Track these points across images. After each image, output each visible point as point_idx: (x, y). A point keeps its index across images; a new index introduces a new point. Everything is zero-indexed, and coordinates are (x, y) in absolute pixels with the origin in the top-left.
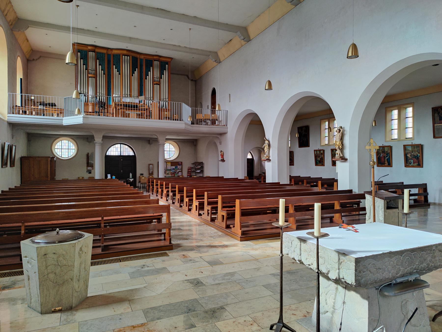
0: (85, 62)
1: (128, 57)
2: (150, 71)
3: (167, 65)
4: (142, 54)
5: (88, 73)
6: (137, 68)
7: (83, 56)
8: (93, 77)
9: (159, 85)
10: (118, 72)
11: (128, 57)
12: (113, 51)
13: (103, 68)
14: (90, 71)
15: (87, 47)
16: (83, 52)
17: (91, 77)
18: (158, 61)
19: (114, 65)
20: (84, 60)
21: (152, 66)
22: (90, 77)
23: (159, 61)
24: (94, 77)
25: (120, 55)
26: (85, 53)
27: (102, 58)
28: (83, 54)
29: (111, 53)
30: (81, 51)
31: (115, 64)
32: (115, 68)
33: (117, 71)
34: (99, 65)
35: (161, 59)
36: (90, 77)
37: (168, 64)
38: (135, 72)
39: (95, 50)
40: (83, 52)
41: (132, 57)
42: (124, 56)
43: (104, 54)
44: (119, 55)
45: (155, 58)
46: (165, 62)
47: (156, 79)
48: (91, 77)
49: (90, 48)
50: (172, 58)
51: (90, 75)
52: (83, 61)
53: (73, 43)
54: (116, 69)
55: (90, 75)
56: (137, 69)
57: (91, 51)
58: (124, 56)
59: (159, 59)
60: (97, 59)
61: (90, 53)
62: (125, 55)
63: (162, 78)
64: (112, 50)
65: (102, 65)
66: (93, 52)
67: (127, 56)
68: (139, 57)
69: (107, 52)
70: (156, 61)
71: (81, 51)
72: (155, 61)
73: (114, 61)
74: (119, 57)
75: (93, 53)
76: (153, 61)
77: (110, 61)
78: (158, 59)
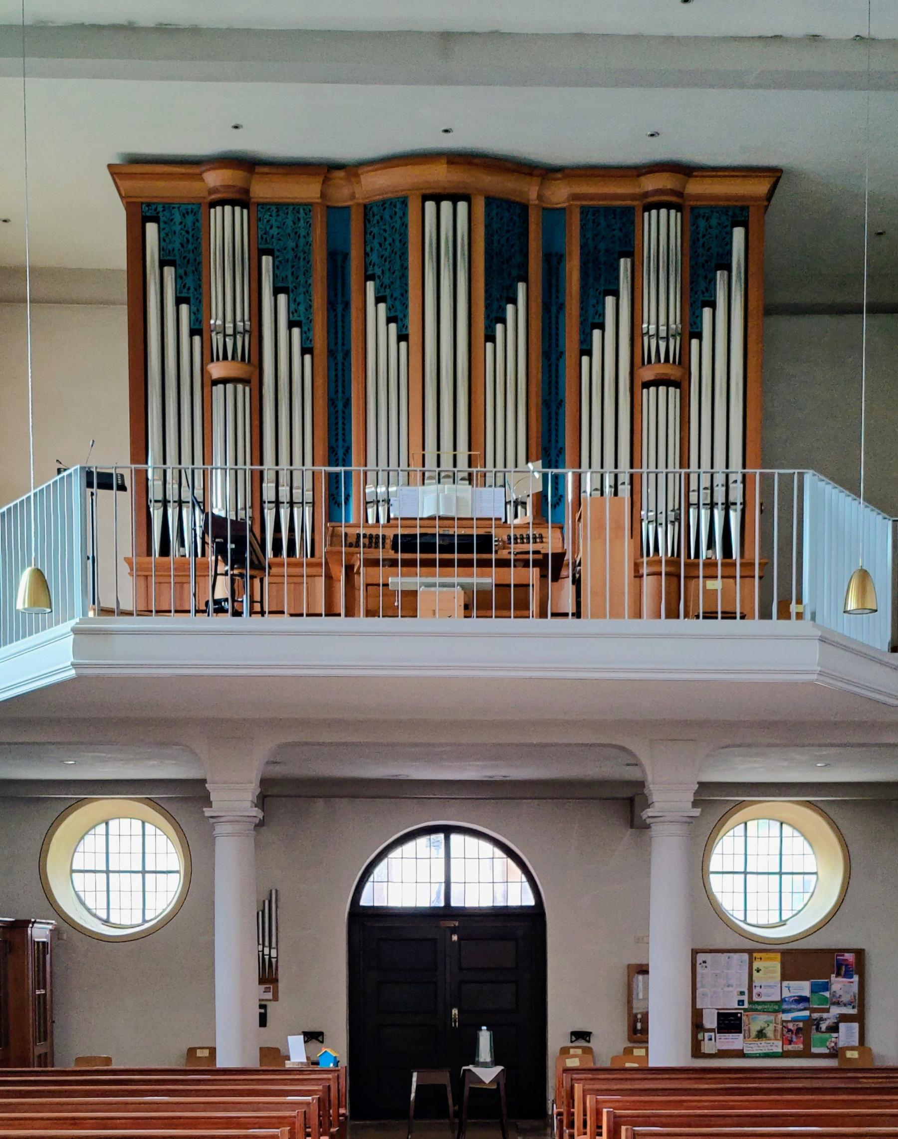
0: (190, 282)
1: (462, 206)
2: (616, 293)
3: (738, 234)
4: (559, 175)
5: (209, 356)
6: (525, 279)
7: (177, 246)
8: (235, 380)
9: (676, 384)
10: (393, 326)
11: (462, 206)
12: (359, 182)
13: (302, 308)
14: (217, 339)
15: (199, 177)
16: (178, 218)
17: (224, 381)
18: (669, 206)
19: (371, 277)
20: (181, 272)
21: (630, 254)
22: (215, 383)
23: (678, 208)
24: (245, 381)
25: (404, 202)
26: (190, 219)
27: (292, 244)
28: (177, 228)
29: (353, 197)
30: (160, 208)
31: (378, 272)
32: (379, 300)
33: (389, 320)
34: (276, 291)
35: (696, 187)
36: (215, 383)
37: (745, 224)
38: (510, 308)
39: (247, 191)
40: (178, 218)
41: (491, 201)
42: (430, 206)
43: (308, 207)
44: (399, 205)
45: (650, 184)
46: (725, 210)
47: (653, 342)
48: (224, 381)
49: (214, 178)
50: (775, 174)
51: (217, 370)
52: (178, 278)
53: (116, 161)
54: (382, 307)
55: (217, 370)
56: (521, 288)
57: (222, 203)
58: (430, 206)
59: (680, 194)
60: (263, 252)
61: (216, 213)
62: (438, 198)
63: (699, 336)
64: (357, 175)
65: (291, 286)
66: (233, 203)
67: (454, 198)
68: (540, 197)
69: (323, 195)
70: (658, 206)
71: (160, 208)
72: (648, 208)
73: (366, 254)
74: (400, 214)
75: (237, 209)
76: (638, 212)
77: (346, 256)
78: (673, 192)
